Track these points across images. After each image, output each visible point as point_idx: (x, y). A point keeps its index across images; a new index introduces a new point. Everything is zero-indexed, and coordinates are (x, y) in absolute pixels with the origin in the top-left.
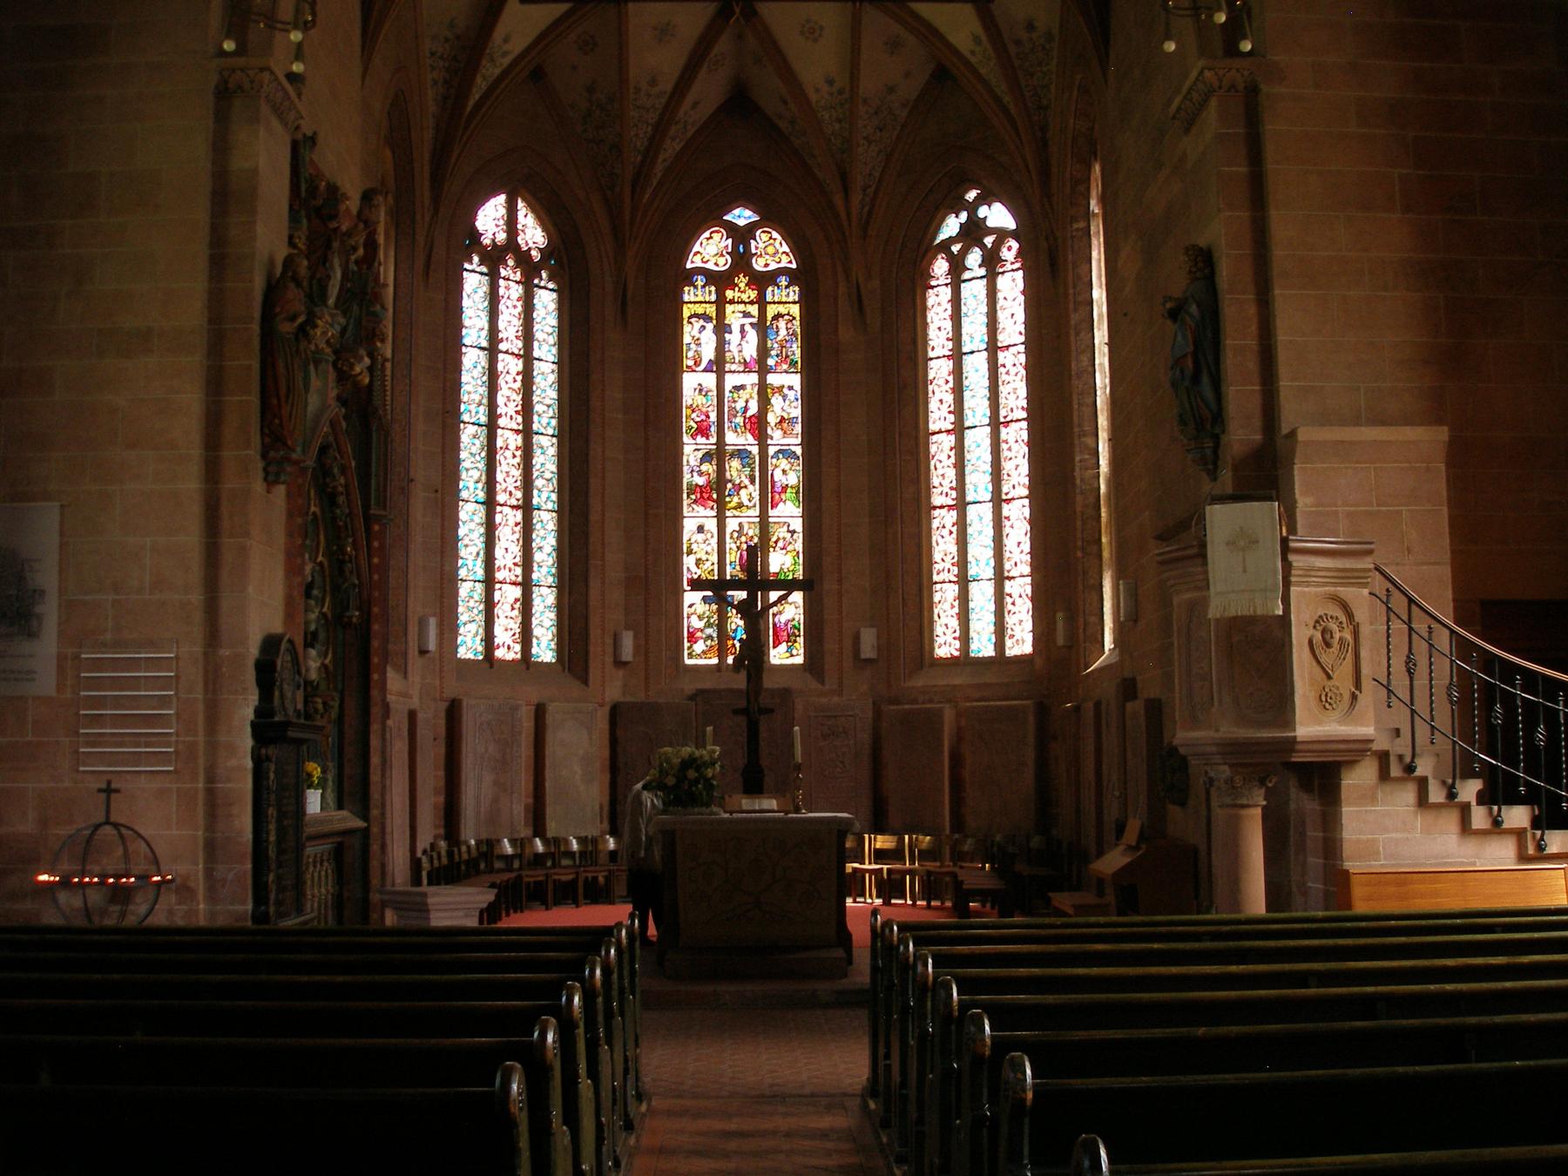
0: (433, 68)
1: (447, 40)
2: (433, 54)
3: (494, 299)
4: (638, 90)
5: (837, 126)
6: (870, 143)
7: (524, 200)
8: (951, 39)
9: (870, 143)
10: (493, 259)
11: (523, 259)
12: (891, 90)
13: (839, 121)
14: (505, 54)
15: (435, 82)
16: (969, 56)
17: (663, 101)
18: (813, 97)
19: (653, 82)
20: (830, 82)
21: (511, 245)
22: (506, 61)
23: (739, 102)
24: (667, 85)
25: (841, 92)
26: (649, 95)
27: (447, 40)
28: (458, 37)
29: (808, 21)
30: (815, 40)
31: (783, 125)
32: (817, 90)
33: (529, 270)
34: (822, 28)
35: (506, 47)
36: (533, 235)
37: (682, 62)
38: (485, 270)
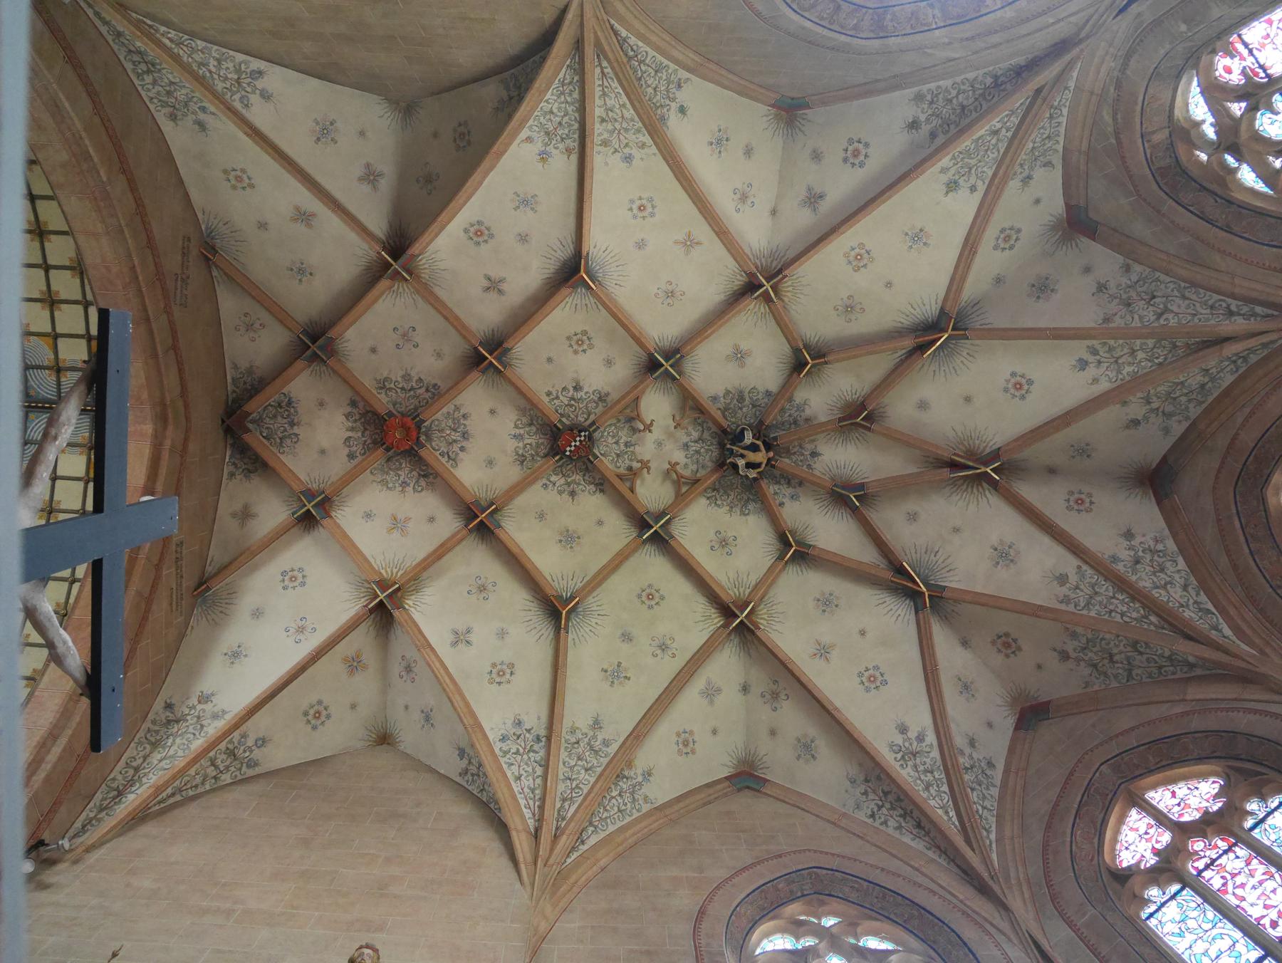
0: (885, 823)
1: (865, 793)
2: (873, 816)
3: (1211, 898)
4: (1066, 600)
5: (1141, 355)
6: (1166, 310)
7: (1154, 787)
8: (970, 219)
9: (1166, 310)
10: (1169, 868)
11: (1208, 825)
12: (1102, 287)
13: (1133, 352)
14: (920, 738)
15: (899, 828)
16: (978, 196)
17: (1090, 571)
18: (1104, 386)
19: (1062, 579)
20: (1083, 365)
21: (1183, 831)
22: (931, 738)
23: (1156, 480)
24: (1070, 564)
25: (1094, 352)
26: (1077, 587)
27: (865, 793)
28: (867, 781)
29: (1006, 390)
30: (1030, 382)
31: (1178, 429)
32: (1095, 381)
33: (1223, 824)
34: (1013, 374)
35: (912, 734)
36: (1196, 796)
37: (1046, 540)
38: (1175, 887)
